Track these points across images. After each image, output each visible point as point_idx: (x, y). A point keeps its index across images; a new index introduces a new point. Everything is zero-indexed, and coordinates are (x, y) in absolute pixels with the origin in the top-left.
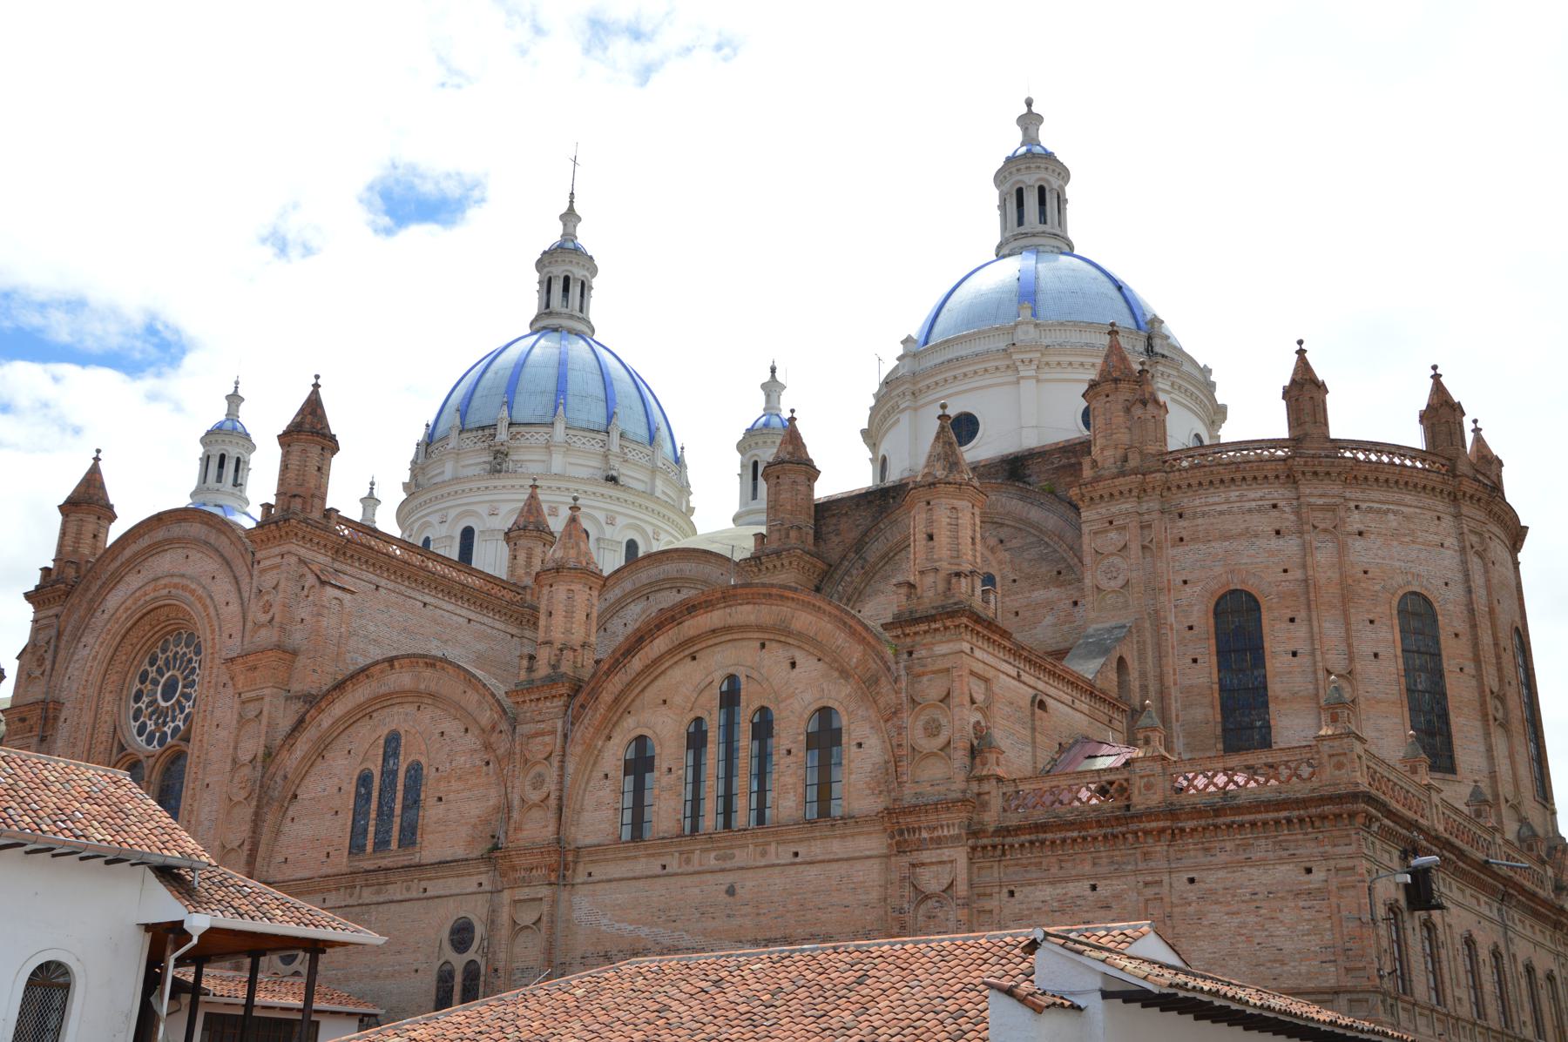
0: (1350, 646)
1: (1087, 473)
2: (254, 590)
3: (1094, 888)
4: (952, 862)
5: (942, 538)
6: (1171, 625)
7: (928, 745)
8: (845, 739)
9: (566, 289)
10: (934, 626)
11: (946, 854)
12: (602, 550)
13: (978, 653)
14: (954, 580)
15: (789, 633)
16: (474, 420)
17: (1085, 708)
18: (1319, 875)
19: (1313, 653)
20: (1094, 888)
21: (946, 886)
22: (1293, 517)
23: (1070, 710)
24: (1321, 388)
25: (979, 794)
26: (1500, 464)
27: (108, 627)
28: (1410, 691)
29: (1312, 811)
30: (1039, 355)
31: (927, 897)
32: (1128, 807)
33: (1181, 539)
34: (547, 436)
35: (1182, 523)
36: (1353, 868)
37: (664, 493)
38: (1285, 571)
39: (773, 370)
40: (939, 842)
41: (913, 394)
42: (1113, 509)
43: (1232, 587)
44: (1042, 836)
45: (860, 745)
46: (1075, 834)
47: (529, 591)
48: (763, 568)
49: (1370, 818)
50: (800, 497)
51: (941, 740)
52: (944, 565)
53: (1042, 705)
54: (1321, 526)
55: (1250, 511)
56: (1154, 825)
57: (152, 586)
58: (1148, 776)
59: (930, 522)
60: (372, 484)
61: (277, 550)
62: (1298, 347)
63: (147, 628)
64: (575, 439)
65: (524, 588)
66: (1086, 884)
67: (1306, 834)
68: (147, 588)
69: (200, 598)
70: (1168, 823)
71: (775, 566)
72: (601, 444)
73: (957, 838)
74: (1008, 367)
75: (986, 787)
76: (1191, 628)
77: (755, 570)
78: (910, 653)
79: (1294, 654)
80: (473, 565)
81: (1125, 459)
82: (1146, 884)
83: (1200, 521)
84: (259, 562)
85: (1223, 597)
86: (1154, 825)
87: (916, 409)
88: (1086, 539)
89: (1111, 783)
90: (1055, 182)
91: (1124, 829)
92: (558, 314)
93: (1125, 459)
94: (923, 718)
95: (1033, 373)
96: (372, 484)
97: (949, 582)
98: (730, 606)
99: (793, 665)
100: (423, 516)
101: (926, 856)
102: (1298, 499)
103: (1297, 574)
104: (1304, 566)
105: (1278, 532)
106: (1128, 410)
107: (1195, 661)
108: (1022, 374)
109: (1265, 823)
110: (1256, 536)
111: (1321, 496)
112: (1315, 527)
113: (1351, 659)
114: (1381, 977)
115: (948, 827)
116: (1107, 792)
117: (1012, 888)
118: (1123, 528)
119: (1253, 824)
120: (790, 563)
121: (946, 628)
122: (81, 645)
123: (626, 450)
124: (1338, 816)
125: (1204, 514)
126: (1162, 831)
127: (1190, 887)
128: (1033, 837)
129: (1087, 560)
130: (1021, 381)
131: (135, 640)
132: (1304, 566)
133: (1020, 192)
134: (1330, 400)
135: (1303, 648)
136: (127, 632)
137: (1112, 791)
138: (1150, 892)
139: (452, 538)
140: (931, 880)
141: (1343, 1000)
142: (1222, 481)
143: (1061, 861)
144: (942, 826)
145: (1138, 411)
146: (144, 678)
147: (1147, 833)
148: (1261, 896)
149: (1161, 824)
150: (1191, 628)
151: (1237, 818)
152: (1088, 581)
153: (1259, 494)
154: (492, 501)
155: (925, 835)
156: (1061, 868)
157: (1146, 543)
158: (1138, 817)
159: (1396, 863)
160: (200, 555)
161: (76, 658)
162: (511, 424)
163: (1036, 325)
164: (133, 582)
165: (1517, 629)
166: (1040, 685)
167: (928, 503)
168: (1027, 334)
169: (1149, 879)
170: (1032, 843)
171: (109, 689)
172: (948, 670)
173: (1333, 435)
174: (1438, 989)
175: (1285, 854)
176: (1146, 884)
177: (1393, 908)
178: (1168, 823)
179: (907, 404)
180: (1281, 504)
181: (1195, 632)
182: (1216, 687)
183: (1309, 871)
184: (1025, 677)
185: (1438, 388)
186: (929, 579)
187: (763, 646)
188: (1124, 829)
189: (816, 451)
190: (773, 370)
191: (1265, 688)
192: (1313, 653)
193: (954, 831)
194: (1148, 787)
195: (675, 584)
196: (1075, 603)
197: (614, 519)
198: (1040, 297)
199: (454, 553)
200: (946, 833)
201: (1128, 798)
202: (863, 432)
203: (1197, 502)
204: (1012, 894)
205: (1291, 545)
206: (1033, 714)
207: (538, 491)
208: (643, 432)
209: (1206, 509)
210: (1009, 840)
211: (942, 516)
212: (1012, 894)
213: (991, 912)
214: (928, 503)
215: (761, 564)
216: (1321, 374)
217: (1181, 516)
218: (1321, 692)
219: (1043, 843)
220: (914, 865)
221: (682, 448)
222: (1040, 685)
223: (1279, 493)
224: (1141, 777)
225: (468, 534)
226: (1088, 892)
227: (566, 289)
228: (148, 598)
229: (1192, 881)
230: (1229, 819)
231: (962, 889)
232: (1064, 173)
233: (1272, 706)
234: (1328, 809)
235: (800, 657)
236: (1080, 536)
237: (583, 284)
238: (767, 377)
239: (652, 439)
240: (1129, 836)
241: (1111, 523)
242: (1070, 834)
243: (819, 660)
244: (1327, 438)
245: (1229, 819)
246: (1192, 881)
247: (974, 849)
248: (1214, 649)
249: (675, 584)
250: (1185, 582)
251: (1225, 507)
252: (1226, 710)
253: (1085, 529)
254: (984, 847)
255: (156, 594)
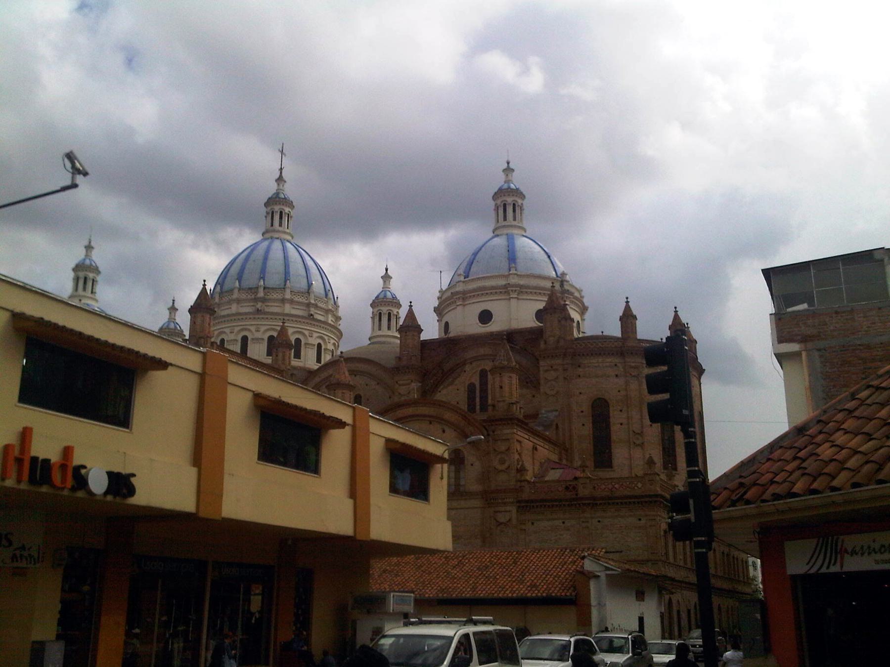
0: (642, 422)
1: (542, 346)
3: (563, 523)
4: (510, 511)
5: (506, 388)
6: (574, 410)
7: (500, 467)
8: (466, 462)
9: (281, 218)
10: (503, 422)
11: (508, 508)
12: (307, 349)
13: (519, 433)
14: (511, 405)
15: (443, 419)
16: (246, 284)
17: (547, 447)
18: (643, 521)
19: (628, 424)
20: (563, 523)
21: (508, 519)
22: (622, 370)
23: (543, 449)
24: (635, 318)
25: (520, 487)
26: (696, 342)
28: (663, 440)
29: (642, 500)
30: (519, 289)
31: (501, 523)
32: (577, 495)
33: (579, 376)
34: (282, 295)
35: (580, 370)
36: (655, 519)
37: (332, 320)
38: (619, 391)
39: (387, 270)
40: (505, 504)
41: (463, 299)
42: (553, 362)
43: (599, 397)
44: (545, 504)
45: (472, 465)
46: (557, 503)
47: (284, 373)
48: (400, 372)
49: (661, 502)
50: (416, 341)
51: (506, 465)
52: (507, 399)
53: (536, 449)
54: (633, 374)
55: (606, 366)
56: (587, 502)
58: (584, 484)
59: (501, 381)
60: (174, 301)
62: (626, 300)
64: (294, 296)
65: (282, 371)
66: (561, 521)
67: (639, 507)
70: (591, 502)
71: (406, 372)
72: (306, 299)
73: (513, 503)
74: (505, 292)
75: (523, 484)
76: (582, 412)
77: (397, 372)
78: (493, 432)
79: (621, 424)
80: (248, 355)
81: (558, 342)
82: (583, 522)
83: (587, 369)
85: (595, 400)
86: (587, 502)
87: (464, 305)
88: (541, 372)
89: (570, 485)
90: (520, 201)
91: (575, 502)
92: (278, 231)
93: (558, 342)
94: (499, 457)
95: (516, 296)
96: (174, 301)
97: (509, 406)
98: (417, 406)
99: (444, 431)
100: (222, 328)
101: (502, 509)
102: (625, 363)
103: (623, 393)
104: (626, 390)
105: (617, 376)
106: (559, 321)
107: (583, 425)
108: (511, 296)
109: (626, 503)
110: (608, 377)
111: (633, 362)
112: (631, 374)
113: (642, 427)
114: (662, 556)
115: (509, 498)
116: (569, 488)
117: (533, 521)
118: (556, 370)
119: (621, 503)
120: (413, 371)
121: (508, 424)
123: (317, 301)
124: (651, 502)
125: (589, 367)
126: (589, 504)
127: (598, 523)
128: (541, 504)
129: (542, 382)
130: (511, 299)
132: (626, 390)
133: (505, 206)
134: (638, 322)
135: (624, 421)
137: (571, 488)
138: (584, 524)
139: (236, 340)
140: (502, 518)
141: (650, 564)
142: (596, 354)
143: (552, 512)
144: (507, 498)
145: (563, 322)
147: (584, 504)
148: (623, 528)
149: (589, 502)
150: (582, 412)
151: (616, 501)
152: (542, 390)
153: (609, 360)
154: (258, 325)
155: (500, 501)
156: (551, 515)
157: (565, 376)
158: (582, 499)
159: (666, 516)
162: (264, 288)
163: (517, 275)
165: (700, 413)
166: (535, 441)
167: (500, 374)
168: (513, 280)
169: (584, 520)
170: (541, 506)
172: (508, 439)
173: (638, 338)
174: (675, 558)
175: (632, 514)
176: (583, 522)
177: (665, 532)
178: (591, 502)
179: (460, 303)
180: (619, 365)
181: (584, 414)
182: (592, 436)
183: (640, 520)
184: (531, 439)
185: (676, 317)
186: (501, 404)
187: (431, 423)
188: (575, 502)
189: (420, 321)
190: (387, 270)
191: (610, 438)
192: (628, 424)
193: (511, 500)
194: (584, 488)
196: (534, 396)
197: (312, 334)
198: (518, 261)
199: (237, 348)
200: (508, 500)
201: (577, 491)
202: (435, 308)
203: (586, 362)
204: (533, 524)
205: (621, 381)
206: (533, 453)
207: (286, 324)
208: (323, 292)
209: (590, 365)
210: (532, 504)
211: (506, 380)
212: (533, 524)
213: (525, 530)
214: (500, 374)
216: (635, 312)
217: (579, 366)
218: (631, 440)
219: (545, 506)
220: (496, 512)
221: (337, 298)
222: (535, 441)
223: (616, 360)
224: (582, 484)
225: (245, 340)
226: (562, 524)
227: (281, 218)
229: (599, 521)
230: (613, 501)
231: (514, 521)
232: (523, 197)
233: (612, 444)
234: (647, 499)
235: (446, 428)
236: (539, 371)
237: (288, 215)
238: (383, 272)
239: (326, 295)
240: (577, 505)
241: (552, 367)
242: (555, 503)
243: (455, 430)
244: (636, 338)
245: (613, 501)
246: (599, 521)
247: (519, 507)
248: (591, 421)
250: (580, 393)
251: (597, 365)
252: (595, 446)
253: (541, 368)
254: (523, 507)
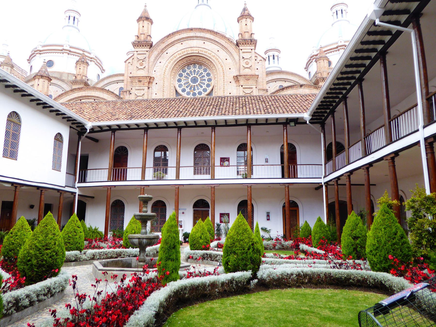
2: (241, 57)
27: (171, 58)
57: (190, 49)
61: (249, 48)
63: (186, 61)
68: (187, 49)
69: (214, 56)
84: (241, 50)
122: (158, 62)
131: (180, 64)
136: (179, 61)
146: (181, 75)
160: (210, 43)
161: (156, 65)
164: (209, 45)
171: (172, 77)
195: (285, 80)
215: (324, 79)
228: (188, 52)
249: (285, 80)
255: (192, 52)
